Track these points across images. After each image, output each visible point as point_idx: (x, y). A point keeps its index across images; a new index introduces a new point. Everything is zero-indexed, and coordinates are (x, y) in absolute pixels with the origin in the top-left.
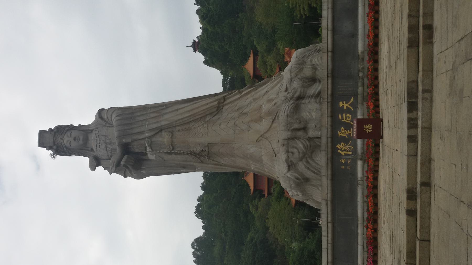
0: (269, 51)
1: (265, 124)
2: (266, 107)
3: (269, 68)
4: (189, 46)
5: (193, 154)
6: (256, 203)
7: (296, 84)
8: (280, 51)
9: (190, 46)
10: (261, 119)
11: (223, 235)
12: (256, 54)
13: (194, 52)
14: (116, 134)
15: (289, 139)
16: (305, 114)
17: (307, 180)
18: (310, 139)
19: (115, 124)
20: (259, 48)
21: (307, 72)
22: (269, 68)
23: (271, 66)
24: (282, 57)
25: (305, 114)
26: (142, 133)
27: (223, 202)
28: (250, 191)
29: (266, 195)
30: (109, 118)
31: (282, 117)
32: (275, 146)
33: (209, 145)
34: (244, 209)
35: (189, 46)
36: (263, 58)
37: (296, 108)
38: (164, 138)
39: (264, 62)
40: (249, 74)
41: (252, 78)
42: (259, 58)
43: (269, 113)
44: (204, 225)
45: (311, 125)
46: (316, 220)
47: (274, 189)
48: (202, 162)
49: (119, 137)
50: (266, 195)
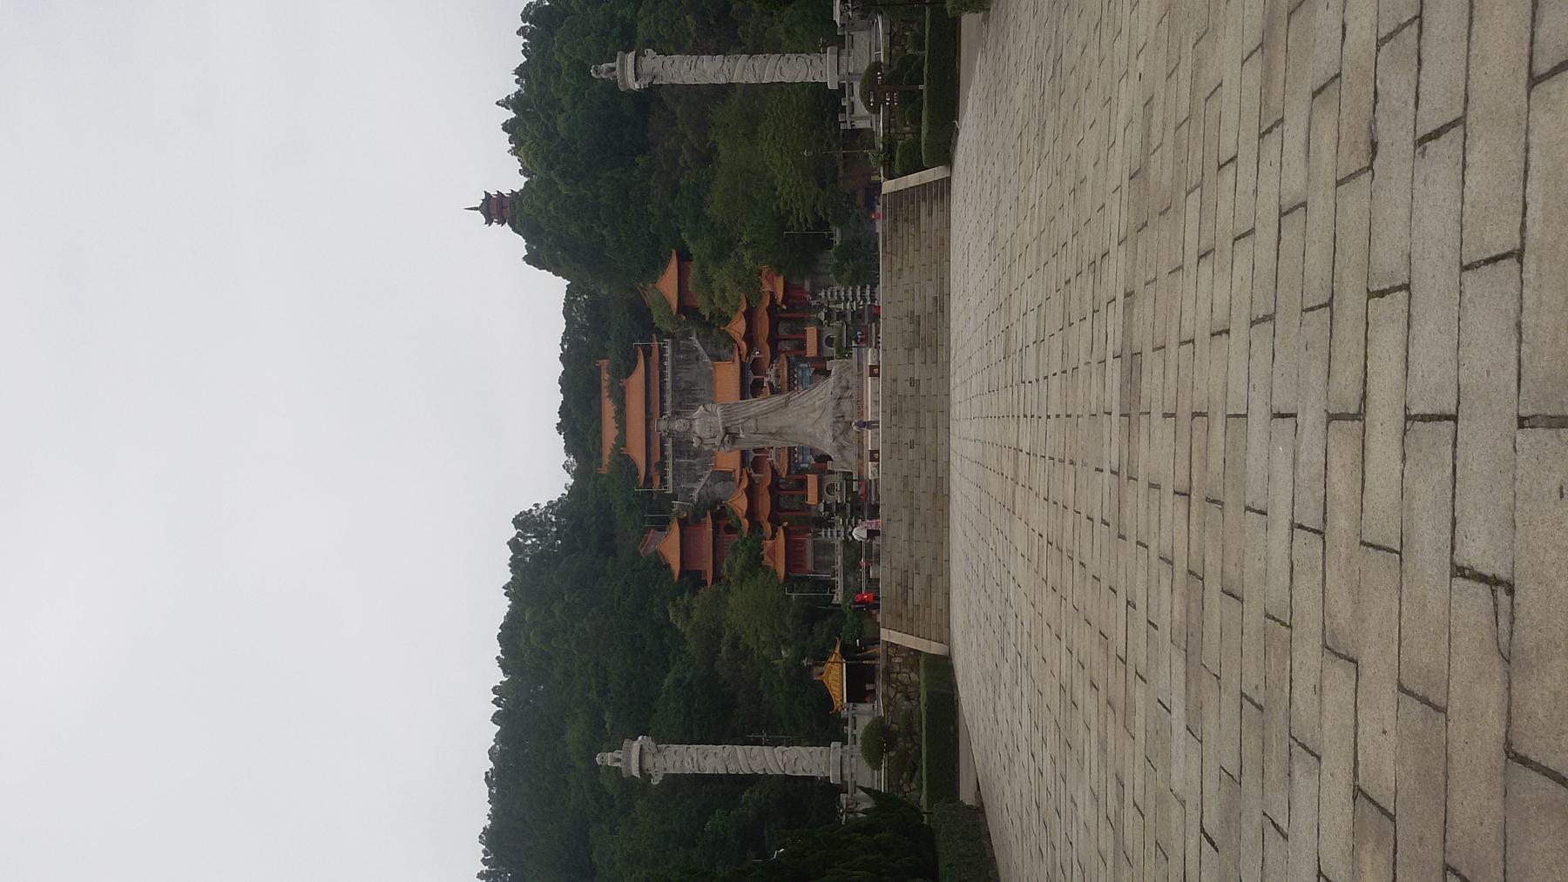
0: (719, 256)
1: (817, 414)
2: (817, 404)
3: (717, 293)
4: (471, 209)
5: (770, 433)
6: (685, 601)
7: (838, 390)
8: (743, 261)
9: (476, 209)
10: (814, 411)
11: (592, 695)
12: (684, 258)
13: (486, 223)
14: (720, 422)
15: (834, 422)
16: (843, 408)
17: (844, 447)
18: (846, 422)
19: (719, 414)
20: (693, 247)
21: (844, 383)
22: (717, 293)
23: (723, 291)
24: (748, 273)
25: (843, 408)
26: (738, 420)
27: (590, 615)
28: (672, 574)
29: (709, 583)
30: (714, 410)
31: (830, 409)
32: (824, 427)
33: (781, 428)
34: (654, 618)
35: (471, 209)
36: (703, 272)
37: (838, 404)
38: (752, 423)
39: (707, 281)
40: (664, 300)
41: (674, 313)
42: (693, 268)
43: (819, 407)
44: (498, 712)
45: (846, 414)
46: (828, 594)
47: (729, 566)
48: (776, 439)
49: (723, 423)
50: (709, 583)
